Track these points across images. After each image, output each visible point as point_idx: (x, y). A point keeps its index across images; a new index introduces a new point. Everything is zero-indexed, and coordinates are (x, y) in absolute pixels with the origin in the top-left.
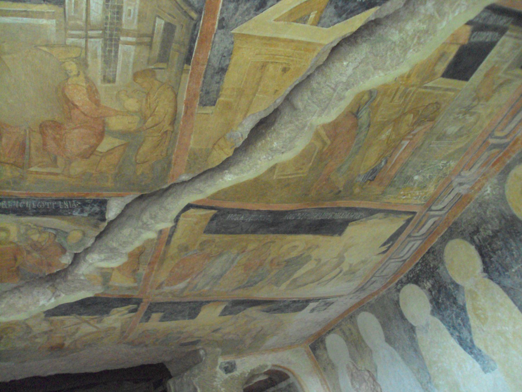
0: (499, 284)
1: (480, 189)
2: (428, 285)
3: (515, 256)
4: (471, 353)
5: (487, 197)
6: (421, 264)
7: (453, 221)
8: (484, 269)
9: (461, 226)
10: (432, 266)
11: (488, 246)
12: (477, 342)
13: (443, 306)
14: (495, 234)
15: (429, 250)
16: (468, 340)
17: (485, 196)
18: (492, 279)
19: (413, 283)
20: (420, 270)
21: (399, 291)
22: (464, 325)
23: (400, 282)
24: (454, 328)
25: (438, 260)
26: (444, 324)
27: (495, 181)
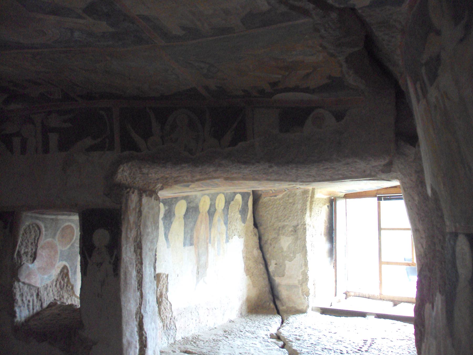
0: (185, 221)
2: (167, 208)
12: (169, 237)
14: (193, 207)
20: (168, 201)
24: (166, 228)
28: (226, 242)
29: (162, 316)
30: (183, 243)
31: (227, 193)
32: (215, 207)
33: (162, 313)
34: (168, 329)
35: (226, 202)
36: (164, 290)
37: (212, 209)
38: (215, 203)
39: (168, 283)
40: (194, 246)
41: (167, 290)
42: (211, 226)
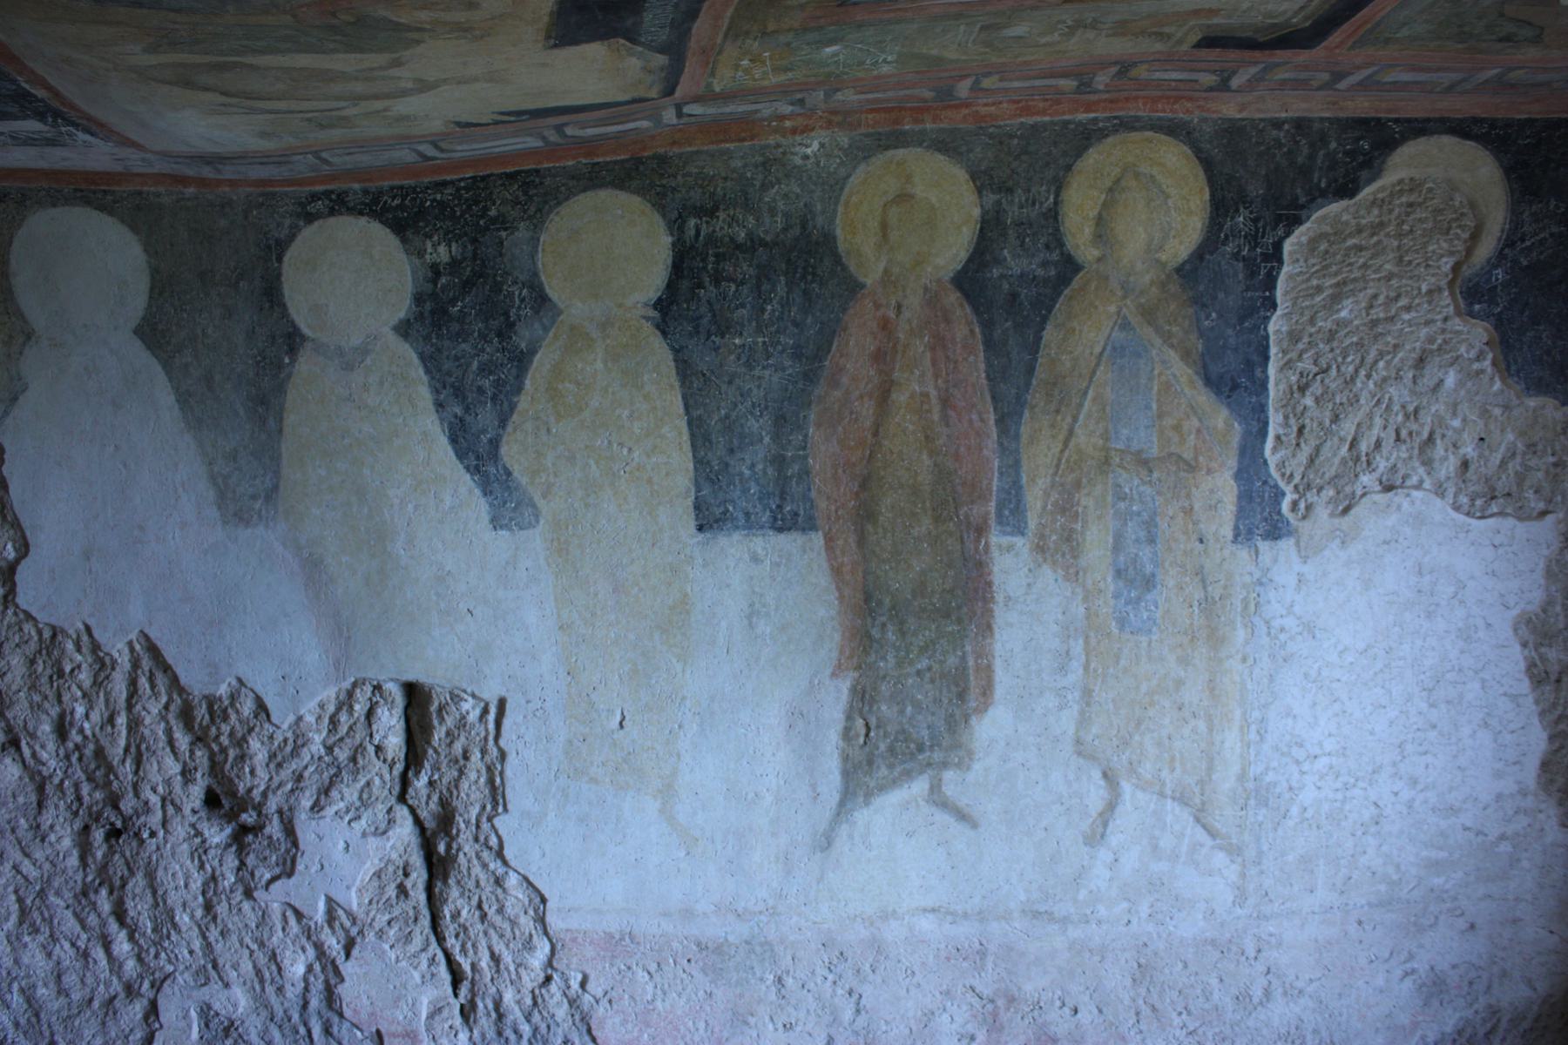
0: (677, 351)
1: (794, 131)
3: (766, 316)
4: (474, 470)
5: (798, 161)
6: (458, 190)
7: (661, 151)
8: (660, 300)
9: (675, 177)
10: (493, 213)
11: (712, 259)
12: (510, 452)
13: (455, 327)
14: (753, 244)
15: (518, 173)
16: (484, 439)
17: (796, 154)
18: (664, 334)
19: (385, 223)
20: (442, 205)
21: (310, 218)
22: (494, 398)
23: (333, 197)
24: (459, 393)
25: (525, 211)
26: (428, 371)
27: (844, 140)
28: (1243, 534)
29: (451, 942)
30: (690, 502)
31: (1233, 131)
32: (1057, 241)
33: (449, 929)
34: (509, 1033)
35: (1220, 208)
36: (472, 794)
37: (1014, 263)
38: (1053, 215)
39: (503, 755)
40: (818, 539)
41: (496, 795)
42: (1020, 402)
